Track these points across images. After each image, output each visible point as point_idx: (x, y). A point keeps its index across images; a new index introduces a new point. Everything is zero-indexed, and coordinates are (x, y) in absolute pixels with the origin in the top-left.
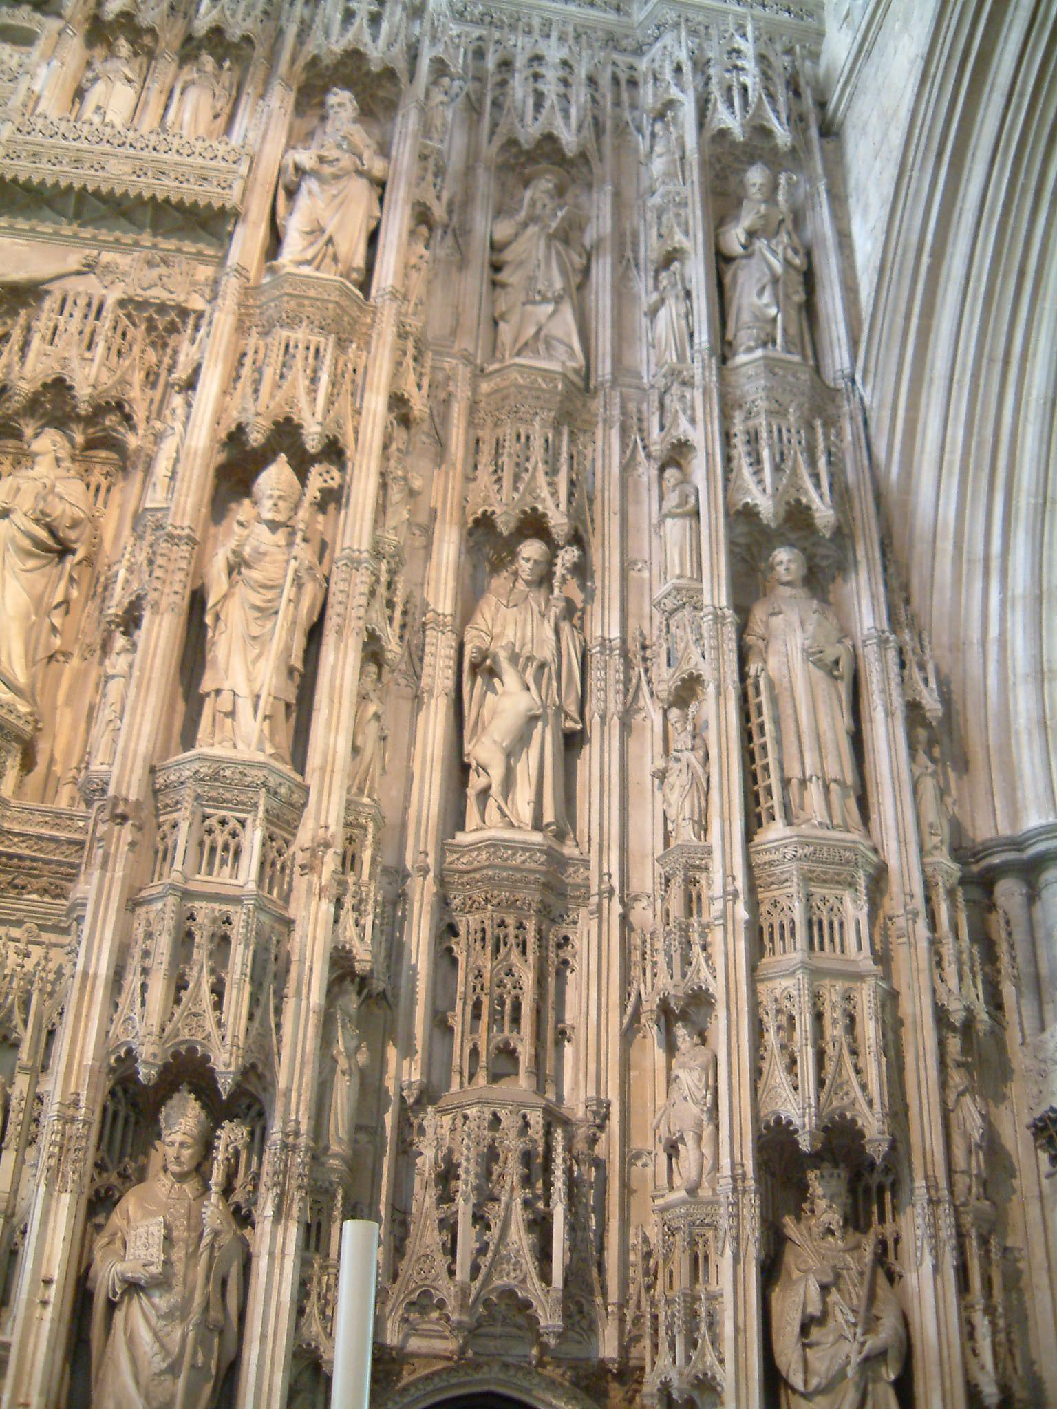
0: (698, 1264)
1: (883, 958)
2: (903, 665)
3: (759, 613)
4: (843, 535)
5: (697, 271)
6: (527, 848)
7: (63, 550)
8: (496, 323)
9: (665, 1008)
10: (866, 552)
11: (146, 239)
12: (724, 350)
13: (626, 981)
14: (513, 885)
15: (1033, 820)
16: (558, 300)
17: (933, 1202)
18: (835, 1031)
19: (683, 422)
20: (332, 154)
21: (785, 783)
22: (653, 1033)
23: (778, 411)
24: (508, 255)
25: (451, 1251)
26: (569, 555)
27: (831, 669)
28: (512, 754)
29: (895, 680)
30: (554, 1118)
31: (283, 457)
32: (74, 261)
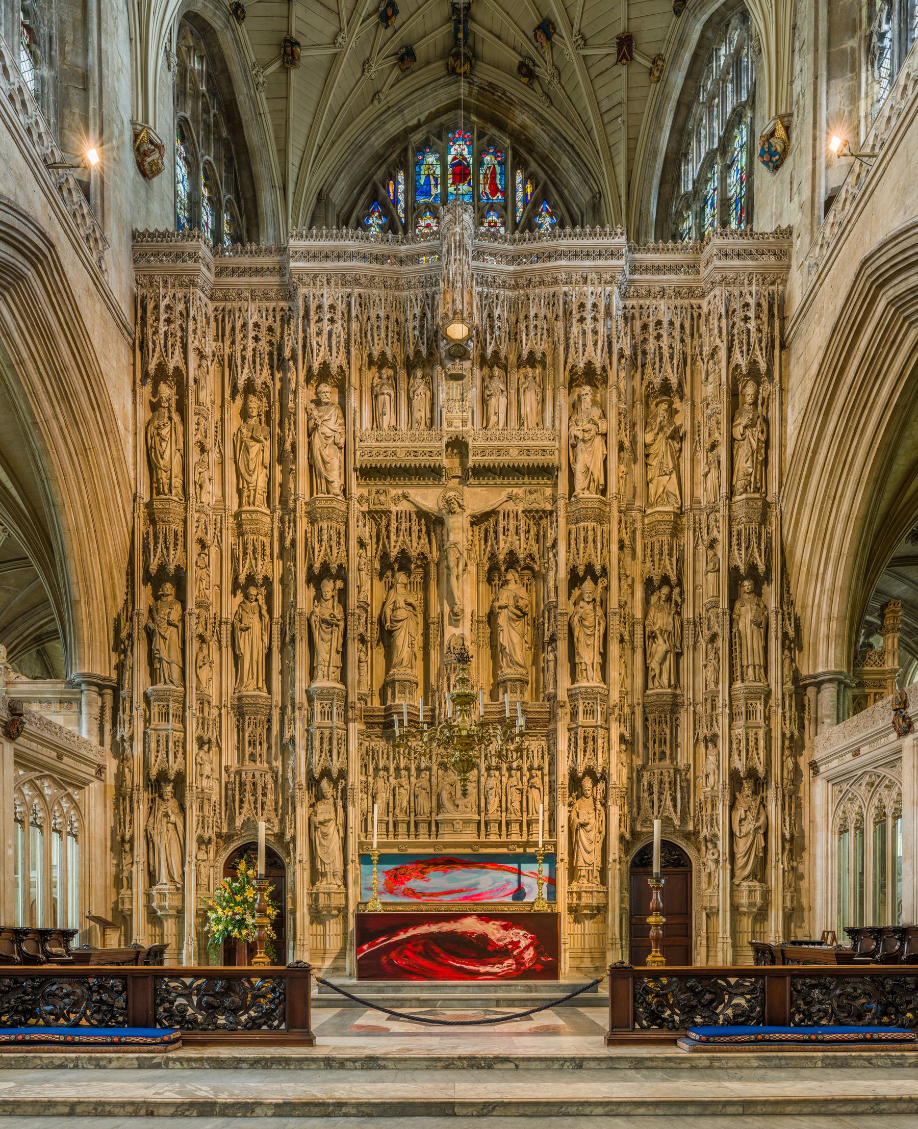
0: (714, 806)
1: (767, 718)
2: (783, 620)
3: (737, 605)
5: (722, 451)
6: (667, 694)
9: (705, 737)
11: (526, 480)
12: (731, 493)
13: (695, 729)
14: (663, 705)
17: (776, 788)
18: (752, 744)
19: (715, 532)
21: (742, 667)
22: (702, 745)
25: (652, 807)
29: (780, 626)
30: (677, 770)
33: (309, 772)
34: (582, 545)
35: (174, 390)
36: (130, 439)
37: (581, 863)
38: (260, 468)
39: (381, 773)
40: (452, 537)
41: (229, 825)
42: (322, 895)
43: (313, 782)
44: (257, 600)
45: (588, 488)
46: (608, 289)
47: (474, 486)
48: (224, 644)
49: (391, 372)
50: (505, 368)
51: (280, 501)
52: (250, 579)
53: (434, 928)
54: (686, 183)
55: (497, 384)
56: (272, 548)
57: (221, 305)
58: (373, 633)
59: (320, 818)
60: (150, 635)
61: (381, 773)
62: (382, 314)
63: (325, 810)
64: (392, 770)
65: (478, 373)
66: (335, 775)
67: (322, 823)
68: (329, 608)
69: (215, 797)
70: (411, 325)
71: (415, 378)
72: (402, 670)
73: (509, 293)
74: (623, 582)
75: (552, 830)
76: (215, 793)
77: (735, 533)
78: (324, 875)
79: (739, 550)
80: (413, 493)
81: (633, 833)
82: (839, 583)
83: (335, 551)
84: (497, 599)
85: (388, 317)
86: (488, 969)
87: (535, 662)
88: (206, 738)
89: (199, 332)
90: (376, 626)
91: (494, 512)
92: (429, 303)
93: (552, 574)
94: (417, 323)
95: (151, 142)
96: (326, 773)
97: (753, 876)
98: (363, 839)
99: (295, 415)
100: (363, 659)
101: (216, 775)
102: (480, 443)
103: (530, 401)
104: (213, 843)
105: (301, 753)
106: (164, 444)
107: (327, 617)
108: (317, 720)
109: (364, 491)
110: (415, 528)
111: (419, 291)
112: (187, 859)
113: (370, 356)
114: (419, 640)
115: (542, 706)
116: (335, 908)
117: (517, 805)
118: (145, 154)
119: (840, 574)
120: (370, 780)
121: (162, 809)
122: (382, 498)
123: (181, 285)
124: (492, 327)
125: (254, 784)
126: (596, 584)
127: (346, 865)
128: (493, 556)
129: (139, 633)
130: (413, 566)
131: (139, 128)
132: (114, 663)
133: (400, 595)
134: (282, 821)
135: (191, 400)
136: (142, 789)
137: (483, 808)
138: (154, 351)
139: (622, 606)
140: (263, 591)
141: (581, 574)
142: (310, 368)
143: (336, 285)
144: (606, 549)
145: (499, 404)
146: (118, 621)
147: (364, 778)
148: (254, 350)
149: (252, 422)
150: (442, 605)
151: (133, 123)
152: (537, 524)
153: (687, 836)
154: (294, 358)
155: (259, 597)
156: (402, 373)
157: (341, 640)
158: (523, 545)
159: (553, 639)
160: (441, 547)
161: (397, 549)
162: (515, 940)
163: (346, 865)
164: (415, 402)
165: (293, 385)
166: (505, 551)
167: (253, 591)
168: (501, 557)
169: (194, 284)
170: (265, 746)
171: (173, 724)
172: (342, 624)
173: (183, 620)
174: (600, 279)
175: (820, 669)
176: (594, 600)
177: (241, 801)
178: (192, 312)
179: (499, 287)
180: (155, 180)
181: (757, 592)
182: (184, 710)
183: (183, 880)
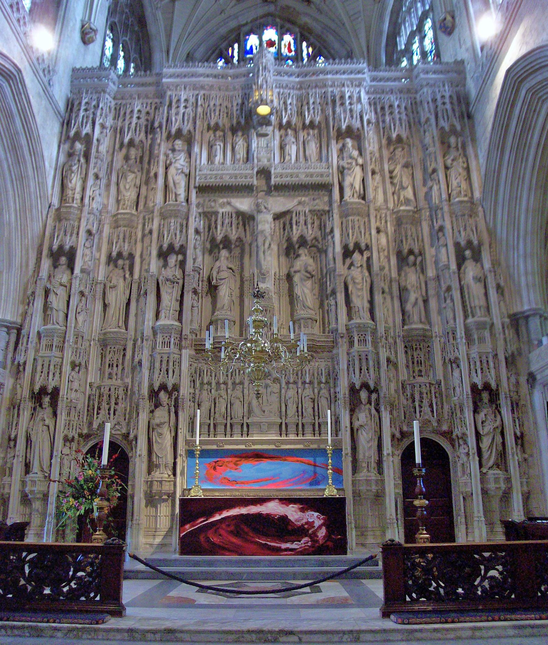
0: (462, 410)
4: (480, 244)
9: (450, 360)
11: (311, 192)
15: (526, 308)
20: (350, 161)
21: (471, 308)
24: (394, 174)
26: (419, 259)
27: (479, 280)
31: (357, 251)
32: (296, 201)
33: (151, 386)
34: (350, 231)
35: (83, 146)
36: (52, 173)
37: (360, 456)
39: (206, 386)
40: (260, 227)
41: (89, 427)
42: (155, 483)
43: (154, 394)
45: (353, 196)
46: (358, 90)
47: (275, 196)
49: (221, 133)
53: (244, 511)
54: (401, 46)
55: (291, 138)
57: (119, 102)
58: (203, 288)
59: (157, 421)
60: (47, 293)
61: (206, 386)
63: (161, 415)
64: (214, 385)
66: (170, 388)
67: (158, 425)
69: (79, 406)
70: (235, 109)
71: (237, 136)
72: (223, 312)
74: (381, 254)
75: (336, 431)
76: (81, 403)
78: (158, 466)
81: (402, 433)
82: (528, 250)
83: (178, 236)
85: (221, 105)
86: (288, 545)
87: (322, 305)
88: (77, 362)
89: (104, 115)
90: (205, 283)
92: (246, 96)
93: (330, 250)
94: (239, 107)
96: (163, 387)
97: (497, 465)
98: (189, 438)
99: (158, 157)
100: (195, 305)
101: (82, 389)
102: (279, 170)
103: (312, 148)
104: (76, 441)
105: (145, 372)
106: (73, 175)
108: (159, 348)
109: (201, 200)
112: (55, 453)
113: (209, 125)
114: (237, 292)
115: (328, 337)
116: (165, 494)
117: (310, 410)
119: (529, 244)
120: (197, 392)
121: (40, 415)
123: (96, 93)
124: (286, 109)
125: (109, 396)
126: (362, 255)
127: (175, 458)
131: (85, 23)
132: (20, 312)
134: (128, 424)
135: (94, 150)
136: (27, 399)
137: (283, 413)
138: (75, 125)
139: (382, 269)
140: (127, 262)
143: (190, 90)
145: (292, 150)
147: (192, 391)
148: (136, 124)
149: (131, 162)
153: (444, 434)
154: (160, 126)
156: (229, 134)
157: (180, 293)
159: (334, 292)
161: (222, 235)
162: (311, 520)
163: (175, 458)
166: (298, 235)
170: (120, 367)
171: (56, 352)
172: (181, 282)
174: (352, 84)
176: (361, 266)
177: (99, 408)
178: (101, 106)
179: (290, 88)
180: (91, 46)
182: (64, 342)
183: (50, 471)
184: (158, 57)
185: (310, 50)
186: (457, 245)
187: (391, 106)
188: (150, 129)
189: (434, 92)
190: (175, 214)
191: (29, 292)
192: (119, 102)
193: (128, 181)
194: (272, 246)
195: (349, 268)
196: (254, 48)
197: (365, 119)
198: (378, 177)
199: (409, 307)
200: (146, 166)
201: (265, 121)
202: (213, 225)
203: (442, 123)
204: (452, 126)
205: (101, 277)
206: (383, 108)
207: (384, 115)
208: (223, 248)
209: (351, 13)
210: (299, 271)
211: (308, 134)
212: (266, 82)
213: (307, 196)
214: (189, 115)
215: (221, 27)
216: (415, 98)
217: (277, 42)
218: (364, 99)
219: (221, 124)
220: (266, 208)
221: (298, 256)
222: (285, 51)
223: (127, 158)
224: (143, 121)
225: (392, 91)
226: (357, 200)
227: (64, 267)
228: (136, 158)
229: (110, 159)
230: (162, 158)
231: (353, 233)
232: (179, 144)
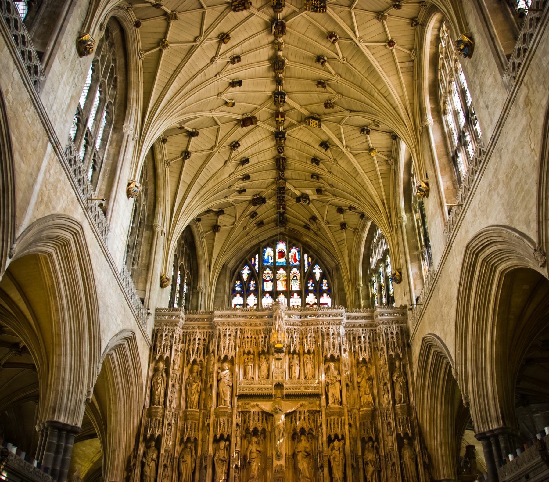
2: (423, 456)
3: (403, 450)
7: (309, 454)
8: (360, 397)
10: (417, 437)
16: (369, 394)
20: (333, 378)
21: (407, 477)
23: (403, 414)
24: (361, 385)
26: (376, 443)
27: (412, 459)
28: (372, 476)
38: (196, 393)
44: (190, 448)
45: (334, 402)
46: (338, 326)
48: (174, 468)
49: (252, 356)
50: (298, 354)
51: (204, 406)
52: (189, 439)
55: (296, 361)
56: (198, 426)
60: (143, 465)
62: (249, 337)
65: (287, 357)
68: (222, 454)
70: (260, 340)
73: (300, 327)
77: (397, 420)
79: (400, 427)
80: (259, 403)
83: (226, 429)
84: (296, 448)
91: (295, 412)
93: (320, 437)
94: (263, 340)
95: (166, 278)
100: (237, 475)
102: (289, 385)
103: (309, 367)
107: (221, 457)
109: (240, 403)
110: (260, 418)
111: (264, 328)
113: (244, 351)
118: (164, 282)
122: (247, 406)
124: (293, 342)
128: (294, 429)
129: (138, 464)
130: (259, 434)
133: (254, 447)
141: (333, 438)
142: (220, 357)
144: (343, 428)
145: (296, 370)
146: (130, 457)
148: (198, 348)
150: (272, 451)
151: (161, 274)
152: (314, 415)
154: (213, 352)
155: (192, 447)
156: (256, 357)
157: (227, 467)
158: (308, 425)
159: (322, 466)
160: (272, 425)
164: (262, 368)
165: (213, 363)
166: (300, 428)
167: (189, 445)
168: (298, 430)
169: (176, 325)
172: (227, 461)
173: (158, 457)
175: (442, 478)
176: (339, 448)
181: (411, 445)
184: (203, 271)
185: (310, 260)
186: (398, 435)
187: (359, 338)
188: (206, 351)
189: (386, 328)
190: (224, 414)
191: (132, 464)
192: (186, 331)
193: (193, 388)
194: (284, 435)
195: (332, 450)
196: (270, 258)
197: (342, 349)
198: (350, 388)
199: (369, 477)
200: (204, 378)
201: (280, 351)
202: (247, 420)
203: (391, 352)
204: (397, 355)
205: (177, 454)
206: (354, 338)
207: (355, 343)
208: (254, 436)
209: (338, 240)
210: (301, 452)
211: (307, 358)
212: (281, 328)
213: (306, 401)
214: (232, 345)
215: (247, 244)
216: (375, 330)
217: (286, 254)
218: (342, 333)
219: (252, 352)
220: (280, 410)
221: (301, 441)
222: (291, 260)
223: (191, 371)
224: (201, 346)
225: (360, 326)
226: (337, 406)
227: (154, 448)
228: (197, 372)
229: (180, 372)
230: (215, 375)
231: (334, 427)
232: (226, 365)
